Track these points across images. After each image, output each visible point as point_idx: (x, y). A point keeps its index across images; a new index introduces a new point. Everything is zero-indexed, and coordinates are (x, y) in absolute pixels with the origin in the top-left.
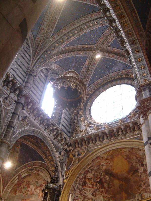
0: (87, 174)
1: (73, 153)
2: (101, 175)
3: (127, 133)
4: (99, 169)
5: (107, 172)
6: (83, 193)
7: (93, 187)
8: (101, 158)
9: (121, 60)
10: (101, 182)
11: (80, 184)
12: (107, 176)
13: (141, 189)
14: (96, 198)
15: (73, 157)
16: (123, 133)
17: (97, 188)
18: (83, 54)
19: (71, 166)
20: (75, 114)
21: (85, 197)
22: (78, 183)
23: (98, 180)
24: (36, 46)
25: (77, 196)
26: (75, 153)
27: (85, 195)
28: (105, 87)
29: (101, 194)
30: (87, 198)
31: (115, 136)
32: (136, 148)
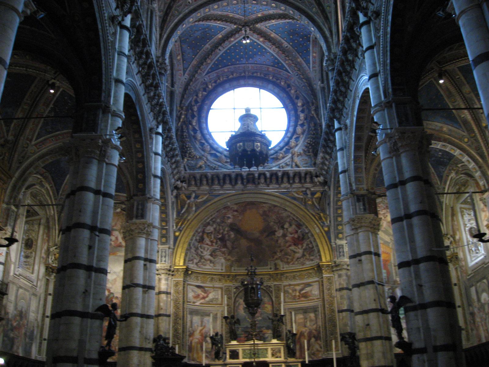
0: (206, 227)
1: (187, 192)
2: (224, 230)
3: (271, 182)
4: (223, 222)
5: (234, 228)
6: (200, 253)
7: (212, 245)
8: (229, 209)
9: (274, 51)
10: (222, 239)
11: (196, 240)
12: (232, 233)
13: (276, 257)
14: (216, 259)
15: (186, 199)
16: (266, 181)
17: (218, 247)
18: (219, 24)
19: (182, 212)
20: (182, 121)
21: (201, 257)
22: (194, 238)
23: (220, 236)
24: (164, 8)
25: (192, 256)
26: (191, 194)
27: (202, 254)
28: (235, 83)
29: (222, 255)
30: (204, 259)
31: (254, 183)
32: (281, 207)
